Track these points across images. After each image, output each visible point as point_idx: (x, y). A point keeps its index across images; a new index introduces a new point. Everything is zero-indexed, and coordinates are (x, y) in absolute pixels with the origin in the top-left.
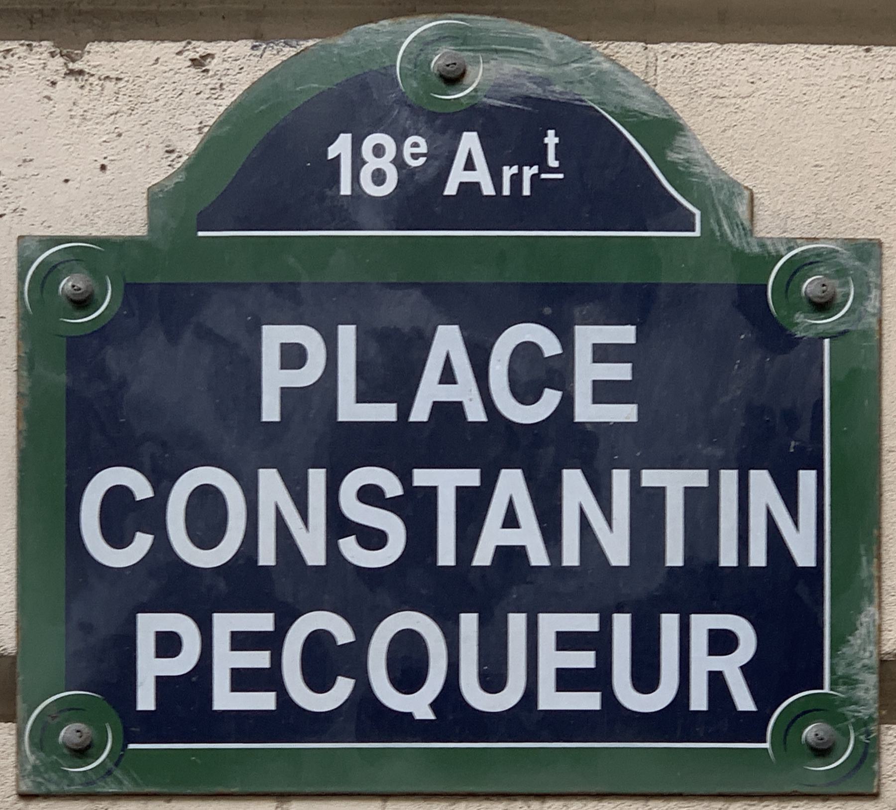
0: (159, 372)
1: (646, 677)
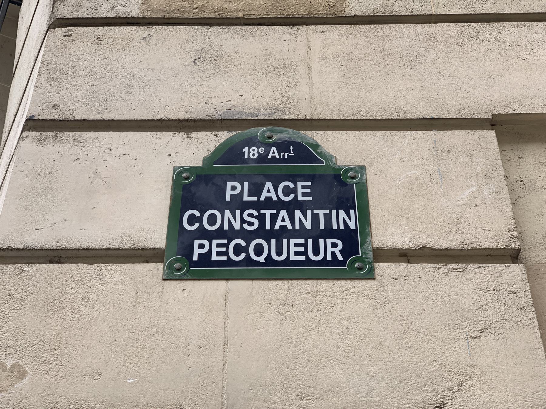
0: (204, 192)
1: (316, 252)
